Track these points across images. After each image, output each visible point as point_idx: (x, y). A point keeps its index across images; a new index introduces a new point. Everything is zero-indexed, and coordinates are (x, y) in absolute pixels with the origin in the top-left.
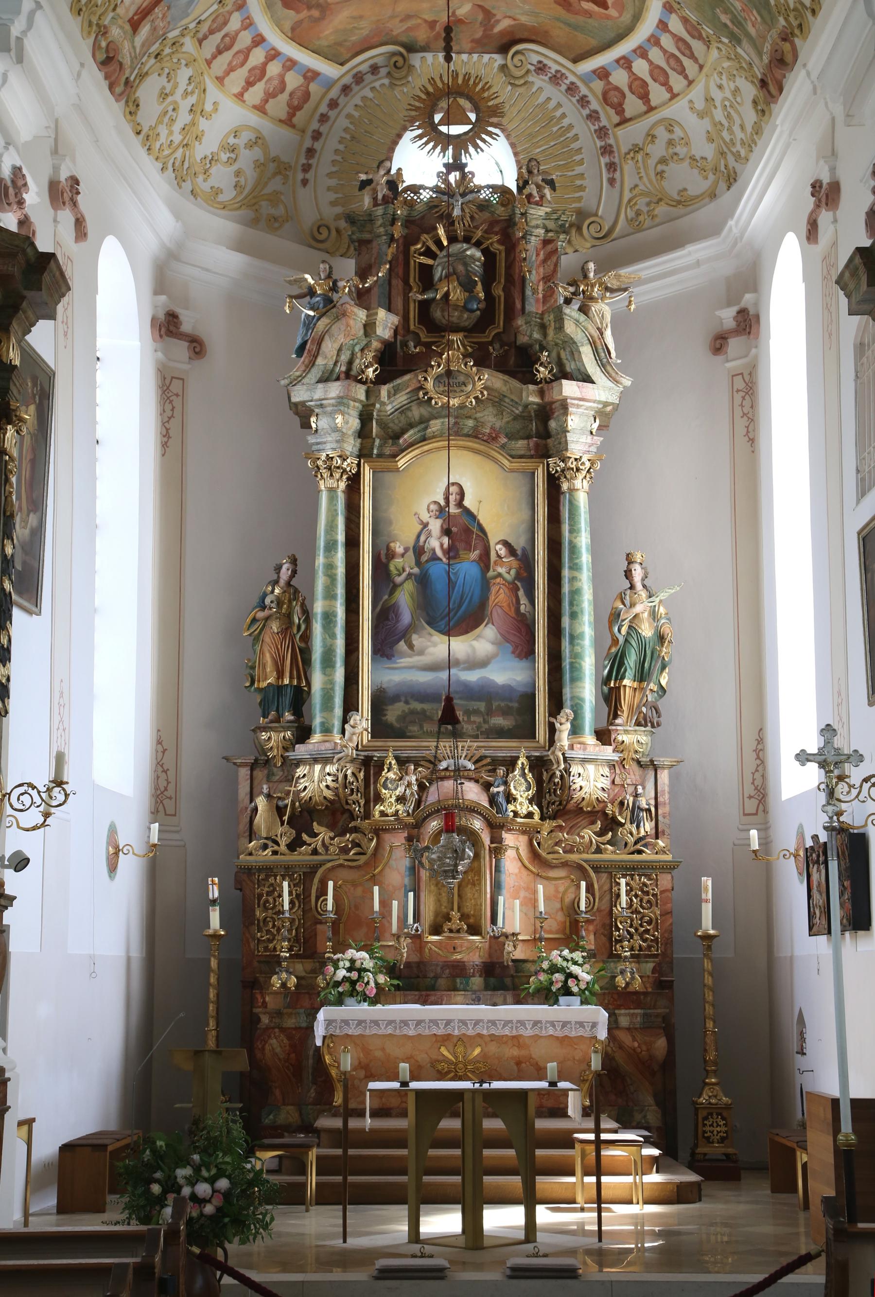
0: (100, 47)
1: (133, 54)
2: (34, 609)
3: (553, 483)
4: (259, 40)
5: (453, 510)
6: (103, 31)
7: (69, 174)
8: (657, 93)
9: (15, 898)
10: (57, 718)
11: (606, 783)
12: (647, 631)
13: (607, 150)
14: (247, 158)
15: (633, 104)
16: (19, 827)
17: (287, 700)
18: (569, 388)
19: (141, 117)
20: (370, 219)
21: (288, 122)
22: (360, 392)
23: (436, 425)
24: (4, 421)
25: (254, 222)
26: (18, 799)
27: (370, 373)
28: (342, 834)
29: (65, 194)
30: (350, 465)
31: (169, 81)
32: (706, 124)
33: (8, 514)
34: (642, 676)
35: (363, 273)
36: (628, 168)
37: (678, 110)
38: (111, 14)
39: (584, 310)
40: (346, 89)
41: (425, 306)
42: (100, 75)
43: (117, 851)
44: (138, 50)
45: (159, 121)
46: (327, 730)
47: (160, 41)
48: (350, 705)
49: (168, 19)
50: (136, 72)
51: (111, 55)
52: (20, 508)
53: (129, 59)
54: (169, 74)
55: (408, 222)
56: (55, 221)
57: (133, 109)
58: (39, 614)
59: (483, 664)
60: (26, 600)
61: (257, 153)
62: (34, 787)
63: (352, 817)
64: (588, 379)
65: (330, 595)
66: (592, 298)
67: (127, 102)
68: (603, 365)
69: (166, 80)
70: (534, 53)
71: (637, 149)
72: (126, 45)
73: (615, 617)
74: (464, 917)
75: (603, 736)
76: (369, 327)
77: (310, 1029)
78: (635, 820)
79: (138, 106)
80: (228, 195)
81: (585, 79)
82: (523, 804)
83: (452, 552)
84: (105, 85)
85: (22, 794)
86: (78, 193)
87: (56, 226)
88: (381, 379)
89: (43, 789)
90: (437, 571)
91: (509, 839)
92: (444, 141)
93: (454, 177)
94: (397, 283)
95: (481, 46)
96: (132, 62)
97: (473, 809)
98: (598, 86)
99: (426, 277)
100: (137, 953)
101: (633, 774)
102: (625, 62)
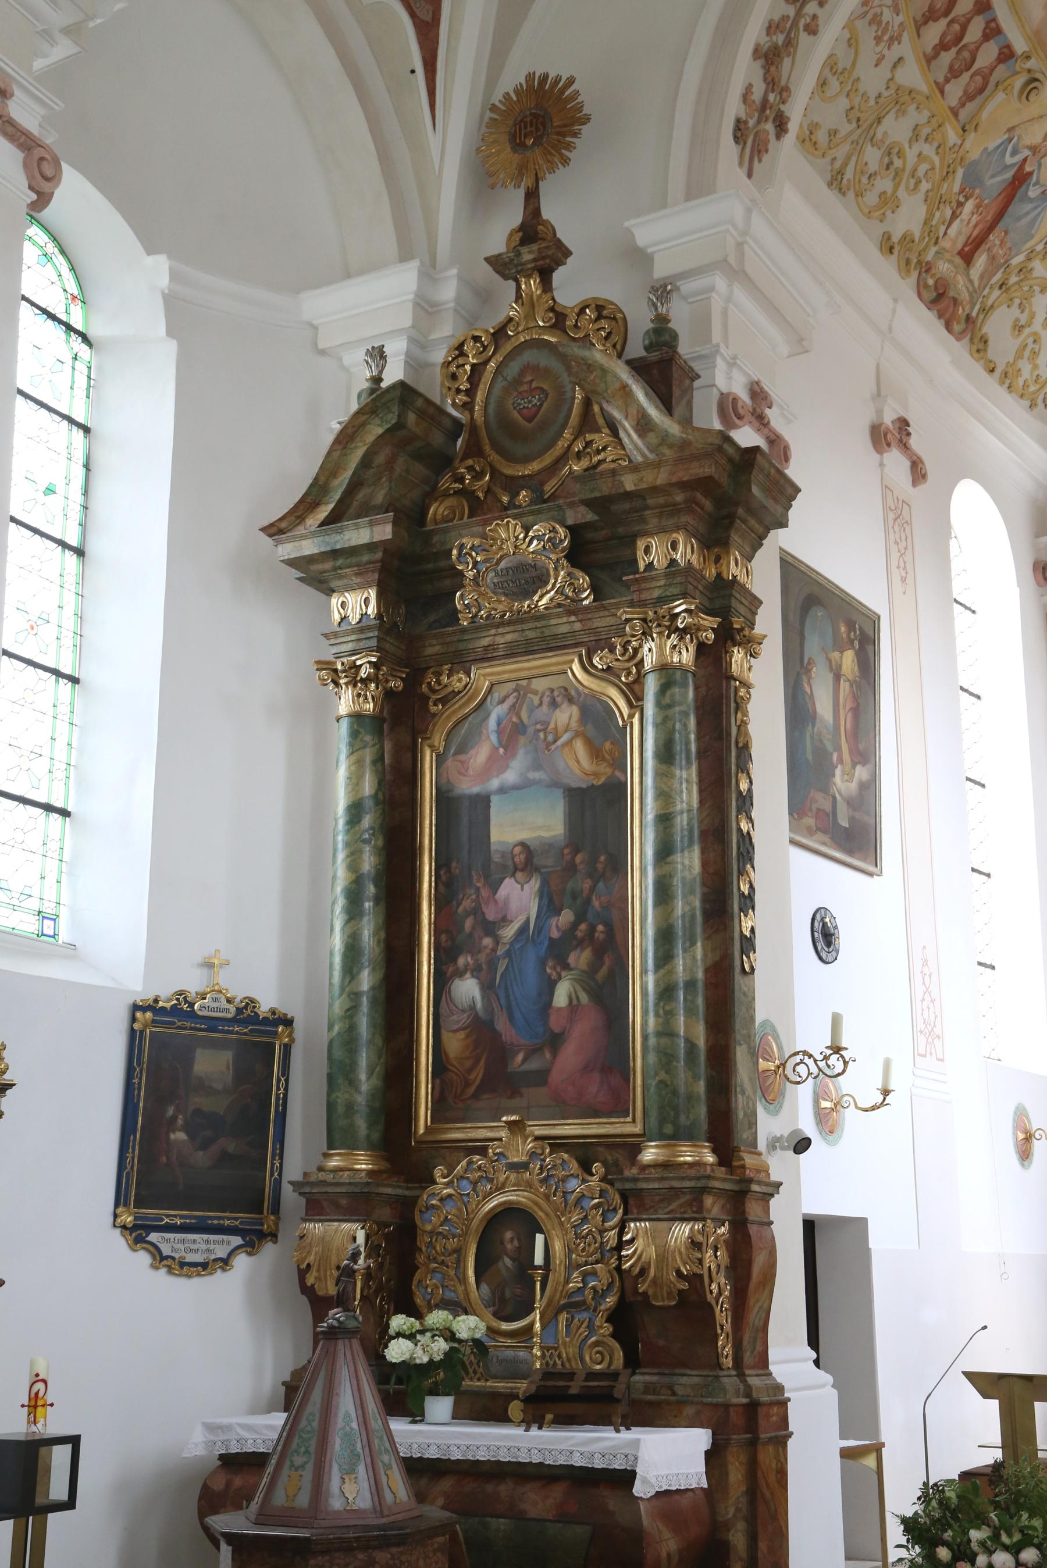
0: (926, 286)
1: (971, 289)
2: (871, 868)
6: (927, 268)
7: (895, 417)
9: (781, 1184)
10: (919, 990)
16: (857, 1107)
19: (991, 354)
24: (729, 643)
26: (794, 1070)
29: (889, 436)
31: (1022, 312)
33: (741, 745)
38: (934, 250)
42: (930, 316)
43: (1029, 1138)
44: (976, 284)
45: (1019, 355)
47: (1002, 270)
49: (1008, 245)
50: (977, 307)
51: (941, 292)
52: (841, 760)
53: (967, 294)
54: (1020, 304)
56: (882, 465)
57: (981, 346)
58: (880, 874)
60: (859, 859)
62: (810, 1056)
67: (971, 340)
69: (1019, 311)
72: (961, 280)
79: (986, 342)
84: (939, 326)
85: (798, 1064)
86: (909, 434)
87: (882, 470)
89: (819, 1057)
96: (971, 295)
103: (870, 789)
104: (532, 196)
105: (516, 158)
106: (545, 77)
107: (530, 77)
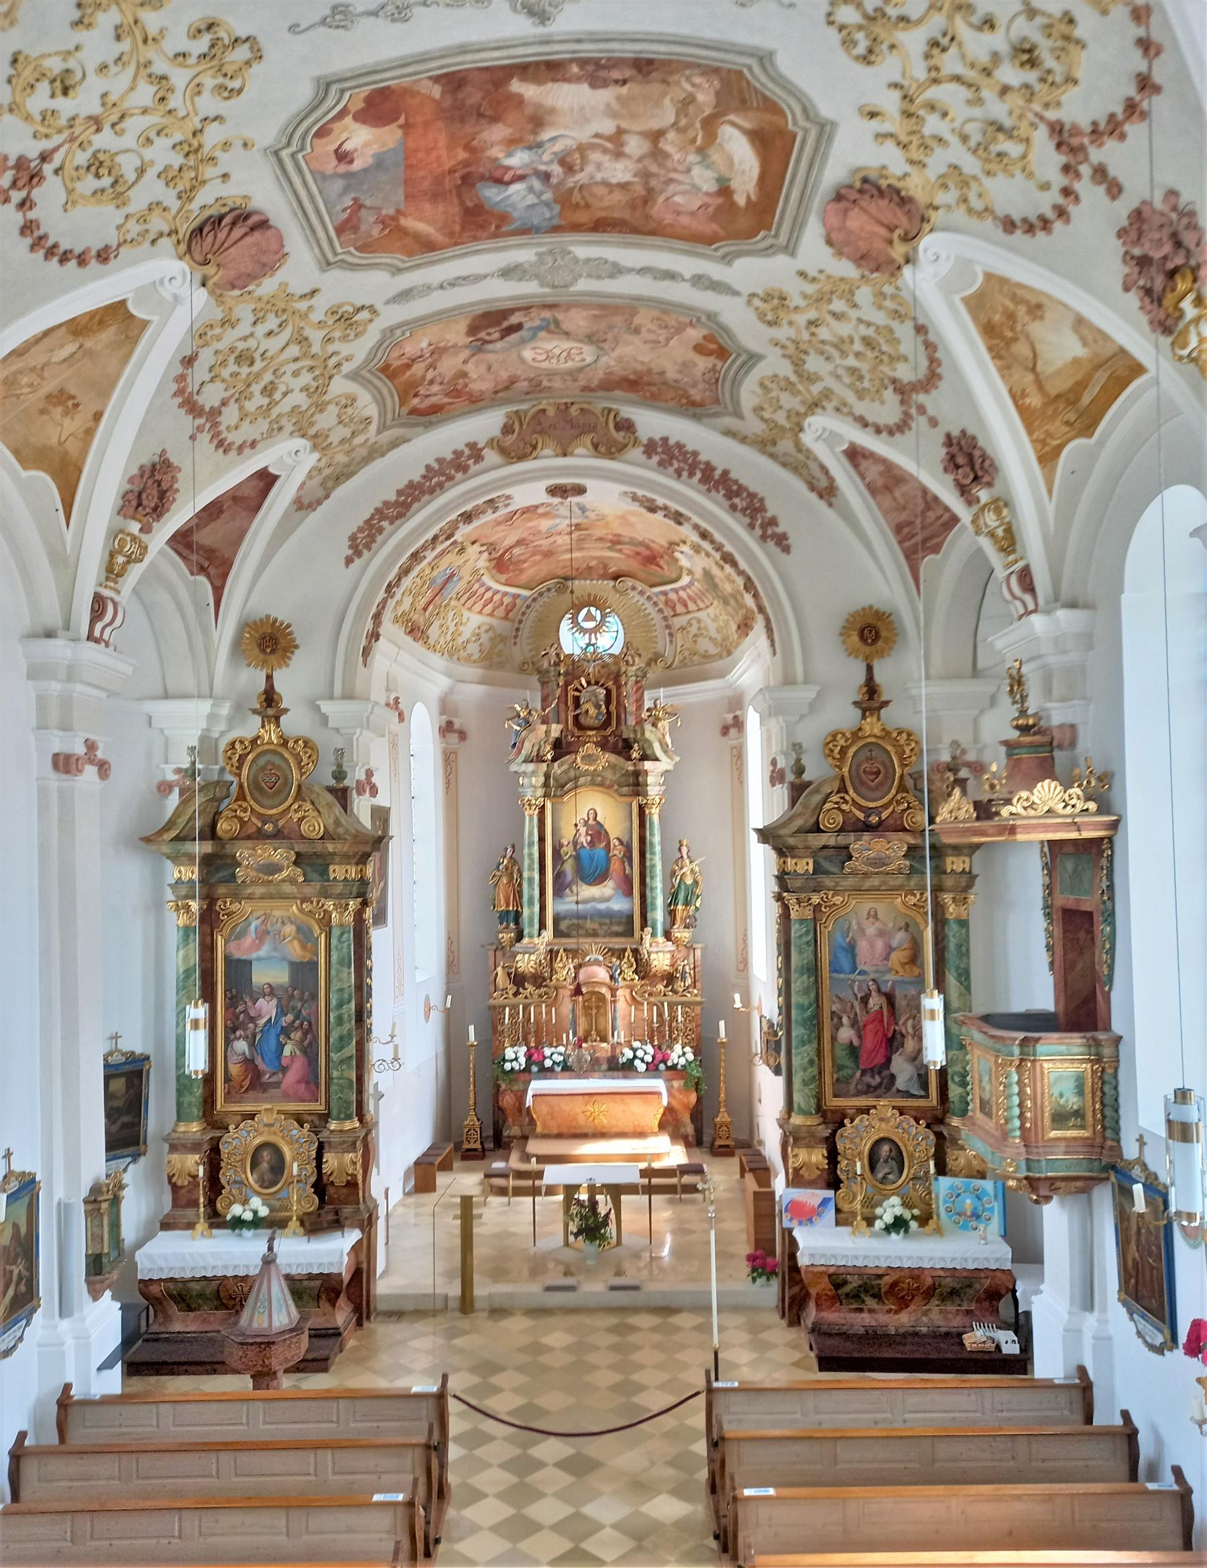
3: (642, 809)
4: (489, 589)
5: (591, 822)
8: (691, 606)
11: (668, 962)
12: (689, 881)
13: (668, 627)
14: (485, 638)
15: (680, 609)
17: (512, 916)
18: (648, 765)
20: (548, 671)
21: (506, 618)
22: (544, 766)
23: (582, 780)
25: (489, 667)
27: (549, 756)
28: (539, 987)
30: (540, 801)
32: (715, 625)
34: (687, 903)
35: (545, 700)
36: (679, 636)
37: (700, 615)
39: (654, 725)
40: (534, 600)
41: (576, 717)
46: (531, 936)
48: (542, 926)
55: (566, 674)
59: (608, 900)
61: (491, 634)
63: (544, 979)
64: (657, 759)
65: (531, 869)
66: (658, 719)
68: (665, 752)
70: (630, 582)
71: (682, 628)
73: (673, 873)
74: (598, 1033)
75: (668, 935)
76: (547, 733)
77: (526, 1091)
78: (683, 979)
80: (476, 656)
81: (656, 594)
82: (629, 973)
83: (592, 844)
88: (554, 760)
90: (583, 853)
91: (619, 993)
92: (583, 631)
93: (591, 649)
94: (562, 706)
95: (604, 577)
97: (602, 984)
98: (663, 598)
99: (577, 702)
100: (441, 1049)
101: (683, 951)
102: (676, 591)
103: (384, 891)
104: (269, 678)
105: (262, 656)
106: (275, 621)
107: (268, 617)
